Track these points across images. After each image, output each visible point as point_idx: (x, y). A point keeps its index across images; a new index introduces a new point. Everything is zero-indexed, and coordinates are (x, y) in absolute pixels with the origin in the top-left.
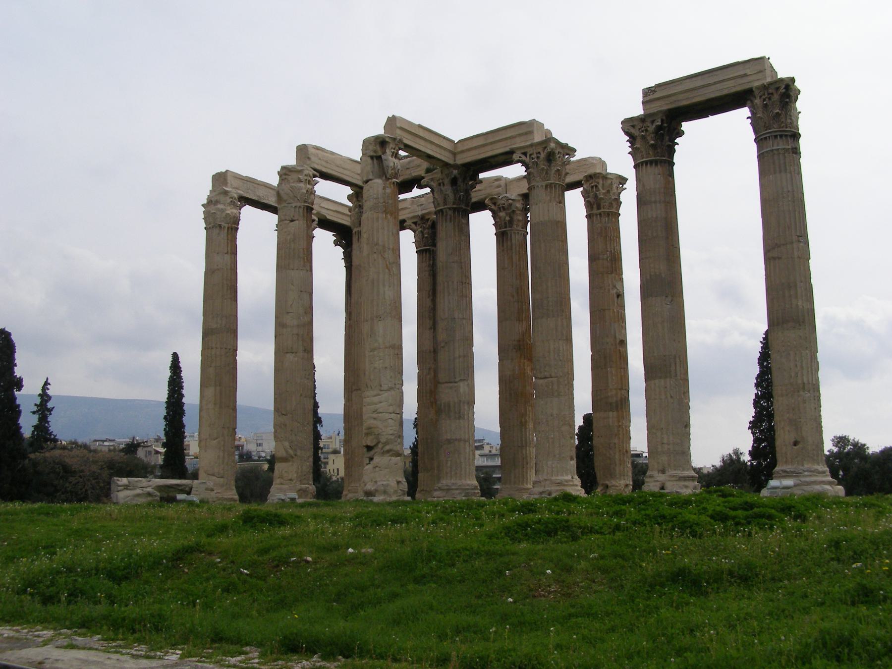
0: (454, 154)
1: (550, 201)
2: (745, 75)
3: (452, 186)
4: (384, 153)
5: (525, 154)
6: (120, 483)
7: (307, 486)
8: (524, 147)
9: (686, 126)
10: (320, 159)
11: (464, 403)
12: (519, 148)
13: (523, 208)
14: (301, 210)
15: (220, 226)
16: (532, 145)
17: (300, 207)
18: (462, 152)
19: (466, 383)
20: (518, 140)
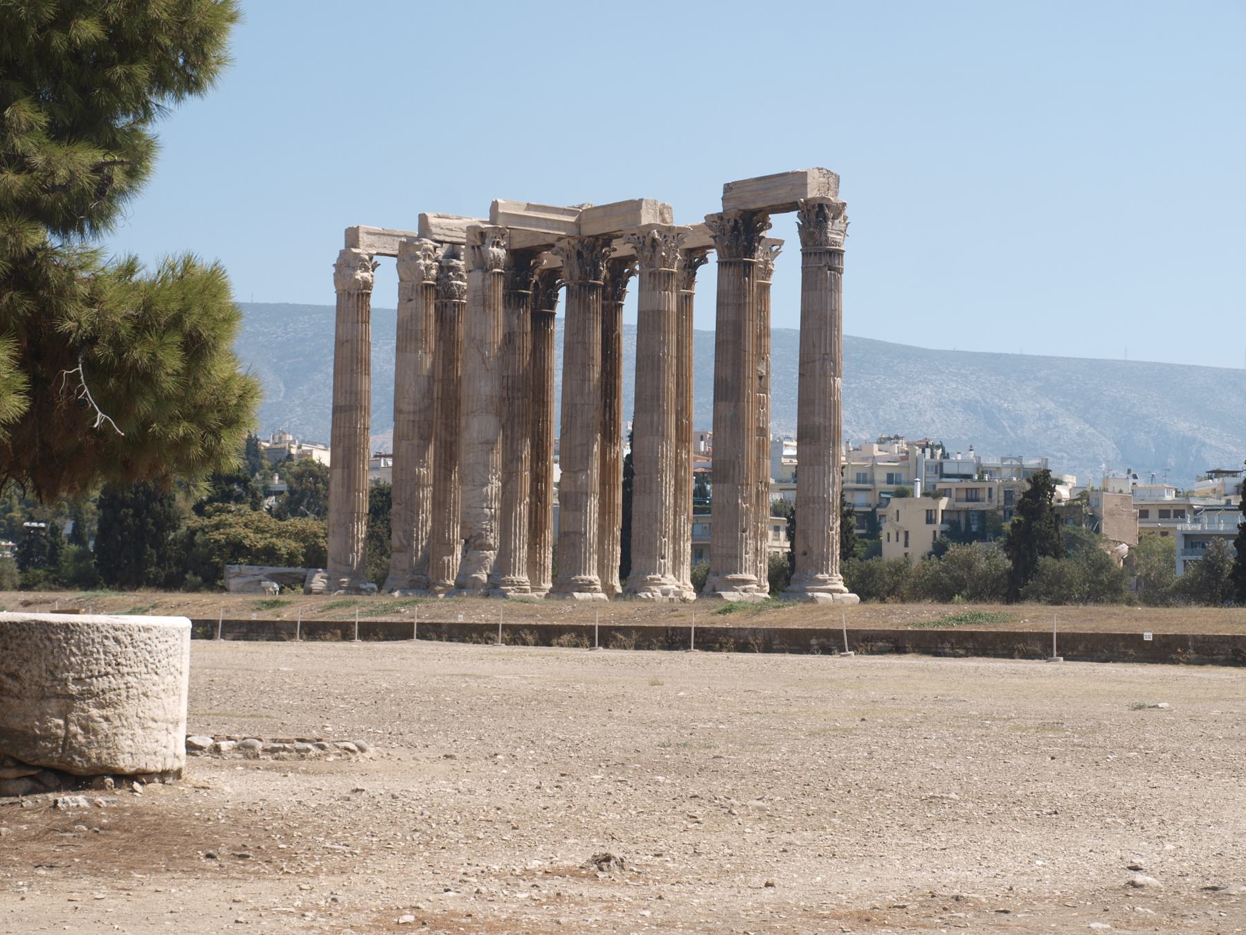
3: (578, 259)
4: (483, 243)
6: (232, 571)
7: (420, 576)
9: (773, 218)
10: (442, 229)
11: (582, 493)
13: (686, 265)
14: (419, 288)
15: (349, 293)
17: (417, 285)
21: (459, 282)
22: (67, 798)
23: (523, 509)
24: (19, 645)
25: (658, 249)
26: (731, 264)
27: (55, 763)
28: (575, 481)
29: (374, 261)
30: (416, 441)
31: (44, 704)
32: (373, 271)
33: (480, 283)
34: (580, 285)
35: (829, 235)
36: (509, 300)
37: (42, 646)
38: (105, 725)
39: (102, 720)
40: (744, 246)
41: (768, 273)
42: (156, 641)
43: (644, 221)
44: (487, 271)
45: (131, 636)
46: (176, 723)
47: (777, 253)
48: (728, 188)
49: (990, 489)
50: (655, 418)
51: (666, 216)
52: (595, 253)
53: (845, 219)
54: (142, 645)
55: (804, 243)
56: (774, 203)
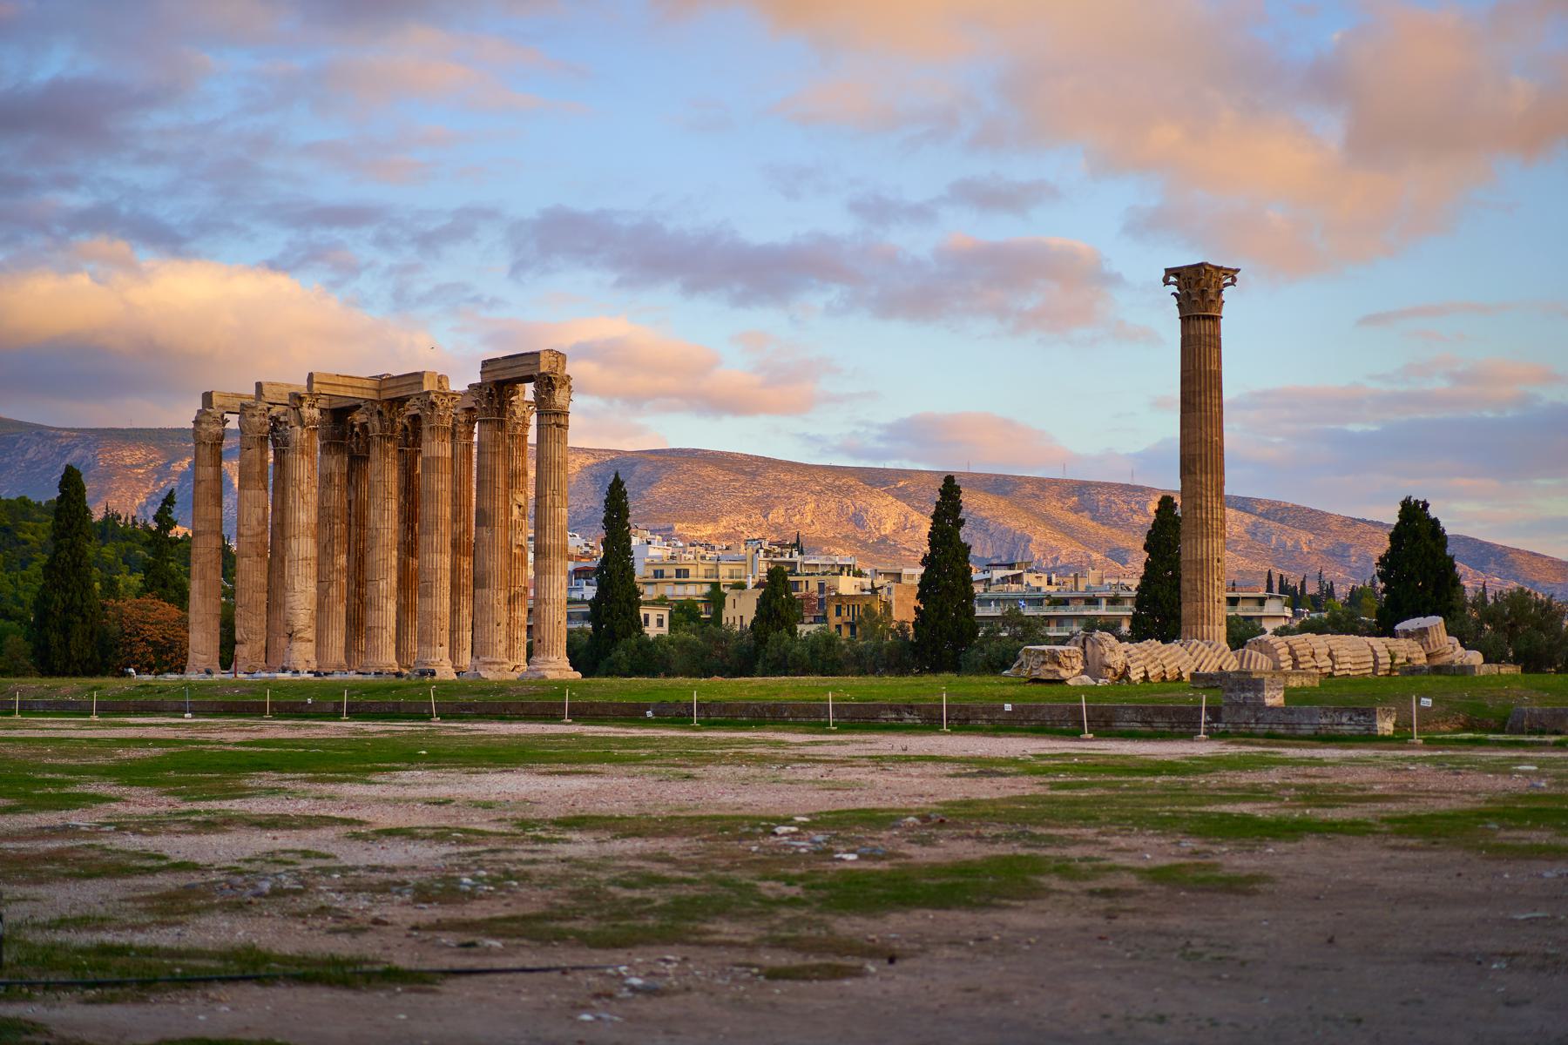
0: (379, 391)
20: (414, 387)
26: (487, 421)
43: (426, 389)
48: (485, 364)
49: (807, 582)
53: (570, 387)
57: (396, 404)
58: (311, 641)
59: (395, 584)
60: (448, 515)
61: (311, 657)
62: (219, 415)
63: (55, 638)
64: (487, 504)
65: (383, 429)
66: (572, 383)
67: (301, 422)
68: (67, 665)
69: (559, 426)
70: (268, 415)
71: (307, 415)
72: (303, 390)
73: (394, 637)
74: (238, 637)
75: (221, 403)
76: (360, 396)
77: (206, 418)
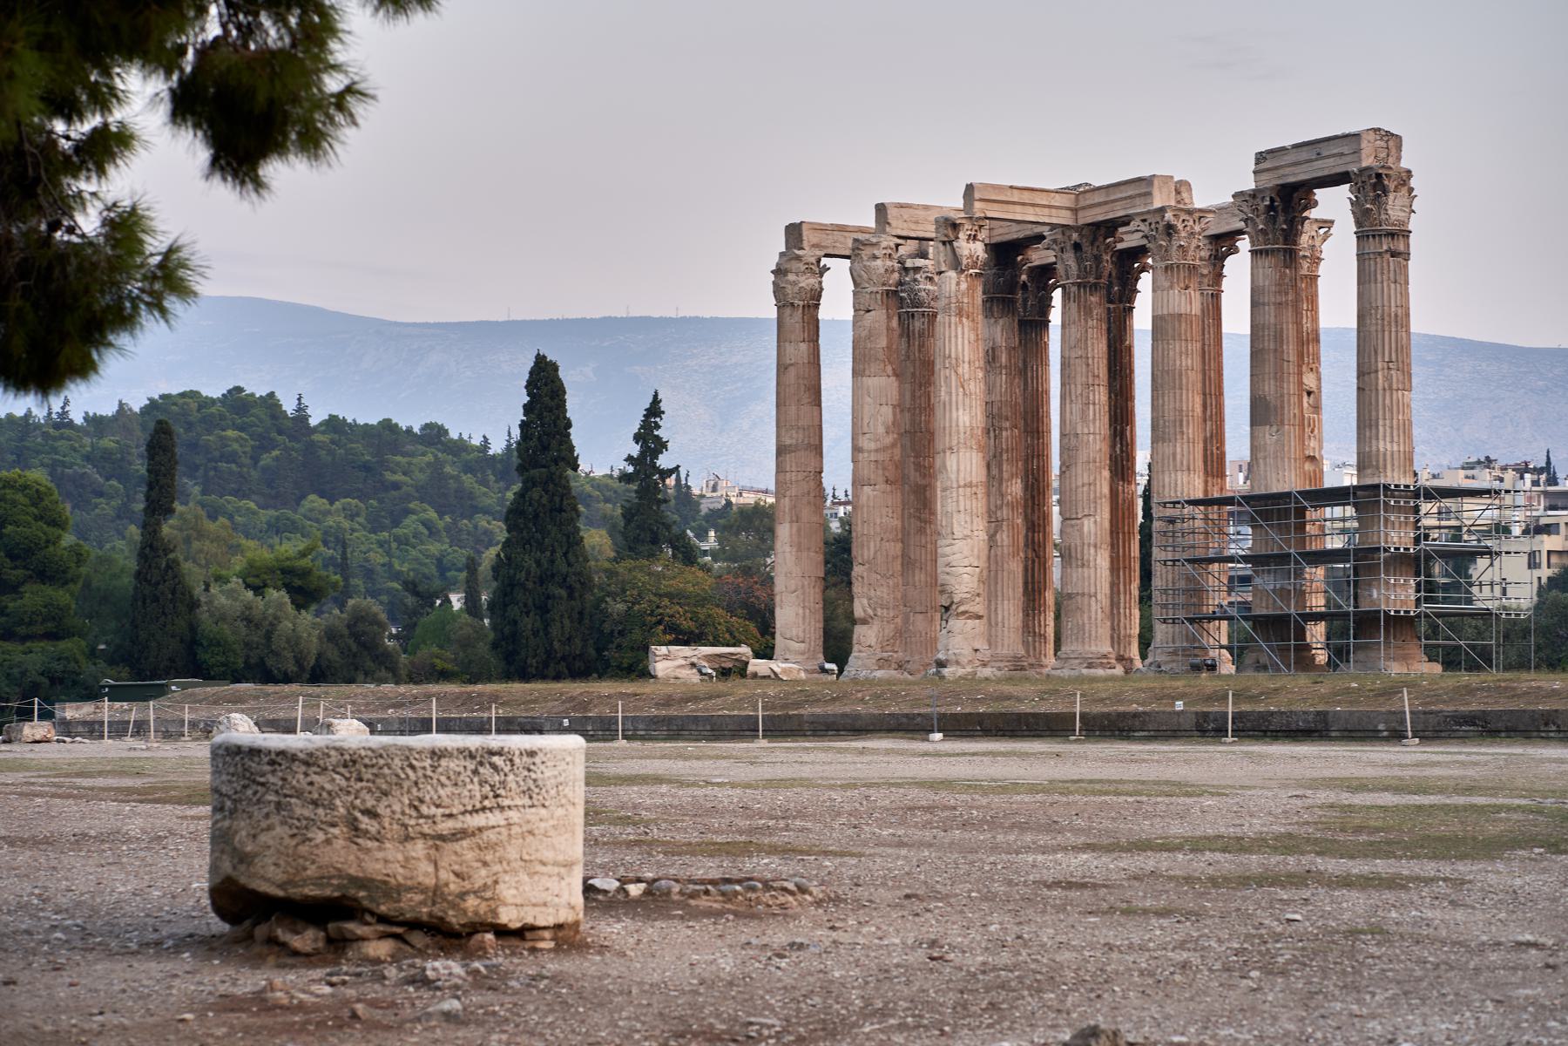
0: (1075, 211)
1: (1171, 287)
2: (1342, 154)
5: (1144, 221)
8: (1142, 213)
9: (1320, 194)
12: (1138, 214)
14: (879, 296)
15: (792, 304)
16: (1148, 212)
18: (1084, 208)
19: (1092, 519)
20: (1137, 201)
21: (929, 287)
22: (437, 964)
23: (1015, 567)
24: (376, 775)
25: (1175, 237)
27: (425, 918)
28: (1081, 531)
29: (822, 264)
30: (881, 486)
31: (409, 846)
32: (821, 276)
33: (953, 287)
34: (1079, 285)
35: (1390, 212)
36: (991, 308)
37: (403, 776)
38: (483, 872)
39: (479, 864)
40: (1283, 230)
41: (1316, 260)
42: (542, 767)
43: (1157, 204)
44: (963, 271)
45: (511, 760)
46: (569, 865)
47: (1326, 237)
48: (1261, 157)
50: (1179, 450)
51: (1185, 195)
52: (1097, 243)
53: (1411, 190)
54: (526, 773)
55: (1358, 223)
56: (1320, 174)
57: (1103, 231)
58: (980, 617)
59: (1107, 525)
60: (1198, 409)
61: (981, 644)
62: (813, 260)
63: (528, 623)
64: (1269, 388)
65: (1082, 272)
66: (1413, 183)
67: (956, 264)
68: (546, 665)
69: (1394, 254)
70: (896, 256)
71: (966, 252)
72: (958, 217)
73: (1107, 610)
74: (858, 612)
75: (815, 241)
76: (1047, 220)
77: (795, 265)
